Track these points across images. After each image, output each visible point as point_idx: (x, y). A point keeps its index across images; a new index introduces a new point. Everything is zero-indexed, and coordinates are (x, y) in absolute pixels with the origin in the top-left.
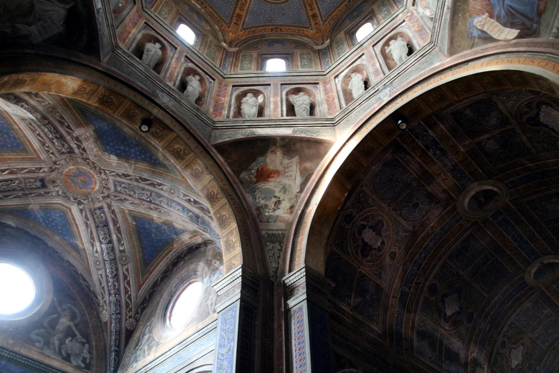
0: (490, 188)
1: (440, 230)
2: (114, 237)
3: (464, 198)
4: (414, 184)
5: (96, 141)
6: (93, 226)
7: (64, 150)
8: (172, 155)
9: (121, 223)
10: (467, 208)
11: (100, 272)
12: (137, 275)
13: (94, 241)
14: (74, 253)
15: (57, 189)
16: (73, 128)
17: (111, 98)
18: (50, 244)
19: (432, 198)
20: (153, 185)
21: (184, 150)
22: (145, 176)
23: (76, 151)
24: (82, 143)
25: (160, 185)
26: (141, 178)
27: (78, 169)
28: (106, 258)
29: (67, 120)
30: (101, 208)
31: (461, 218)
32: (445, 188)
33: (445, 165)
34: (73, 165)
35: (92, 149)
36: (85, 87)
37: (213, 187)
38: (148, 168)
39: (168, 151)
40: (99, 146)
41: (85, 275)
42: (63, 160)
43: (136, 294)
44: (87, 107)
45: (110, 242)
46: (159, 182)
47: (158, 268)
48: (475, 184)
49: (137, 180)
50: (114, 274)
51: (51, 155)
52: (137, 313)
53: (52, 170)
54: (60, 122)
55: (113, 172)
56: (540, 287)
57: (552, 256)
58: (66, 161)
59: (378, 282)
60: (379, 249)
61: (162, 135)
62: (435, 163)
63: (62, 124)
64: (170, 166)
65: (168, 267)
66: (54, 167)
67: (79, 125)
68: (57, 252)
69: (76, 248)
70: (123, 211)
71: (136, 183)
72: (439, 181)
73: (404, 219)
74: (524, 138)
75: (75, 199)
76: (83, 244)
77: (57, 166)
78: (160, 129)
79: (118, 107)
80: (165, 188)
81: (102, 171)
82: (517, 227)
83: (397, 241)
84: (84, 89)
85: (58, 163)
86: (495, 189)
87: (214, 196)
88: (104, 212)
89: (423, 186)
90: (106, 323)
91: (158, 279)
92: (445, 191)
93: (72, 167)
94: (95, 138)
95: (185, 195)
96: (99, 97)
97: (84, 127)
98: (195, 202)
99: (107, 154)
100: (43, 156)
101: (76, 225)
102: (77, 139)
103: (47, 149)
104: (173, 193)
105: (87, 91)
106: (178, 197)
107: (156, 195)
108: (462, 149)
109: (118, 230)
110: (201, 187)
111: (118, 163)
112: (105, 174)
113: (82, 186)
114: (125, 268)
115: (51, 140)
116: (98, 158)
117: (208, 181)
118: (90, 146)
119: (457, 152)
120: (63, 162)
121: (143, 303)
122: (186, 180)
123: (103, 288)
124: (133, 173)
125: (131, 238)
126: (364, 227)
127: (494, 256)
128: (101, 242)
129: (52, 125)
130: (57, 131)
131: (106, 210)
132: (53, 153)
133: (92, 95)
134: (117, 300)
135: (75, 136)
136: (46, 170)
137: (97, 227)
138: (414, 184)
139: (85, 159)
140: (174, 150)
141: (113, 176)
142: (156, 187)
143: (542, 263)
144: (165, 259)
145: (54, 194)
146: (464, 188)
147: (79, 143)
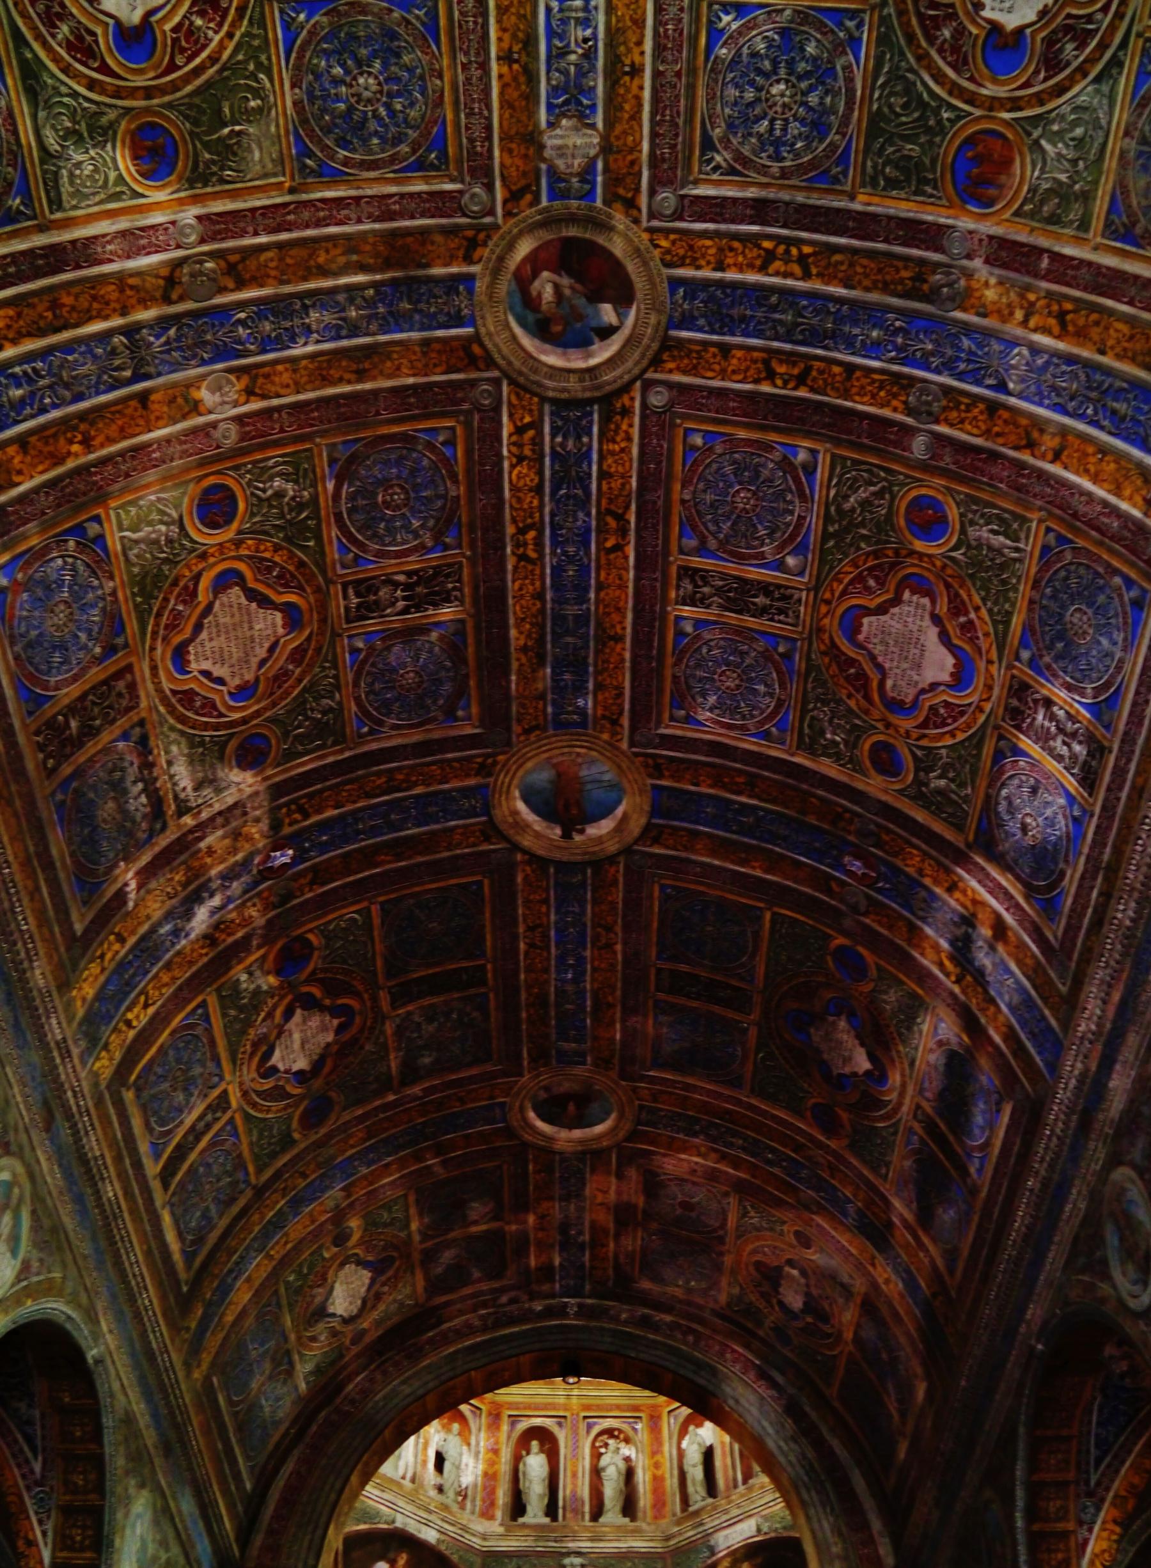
0: (540, 1124)
1: (695, 1134)
3: (599, 1137)
4: (654, 1226)
10: (613, 1116)
19: (652, 1184)
31: (641, 1107)
32: (613, 1180)
33: (580, 1209)
48: (558, 1146)
56: (632, 744)
57: (526, 842)
59: (859, 1300)
60: (803, 1273)
62: (594, 1226)
72: (612, 1196)
73: (725, 1220)
74: (414, 1226)
82: (552, 997)
83: (771, 1229)
86: (531, 1115)
89: (644, 1211)
92: (620, 1176)
108: (531, 1219)
119: (542, 1217)
126: (781, 1303)
127: (659, 971)
138: (654, 1226)
143: (566, 835)
146: (583, 1153)
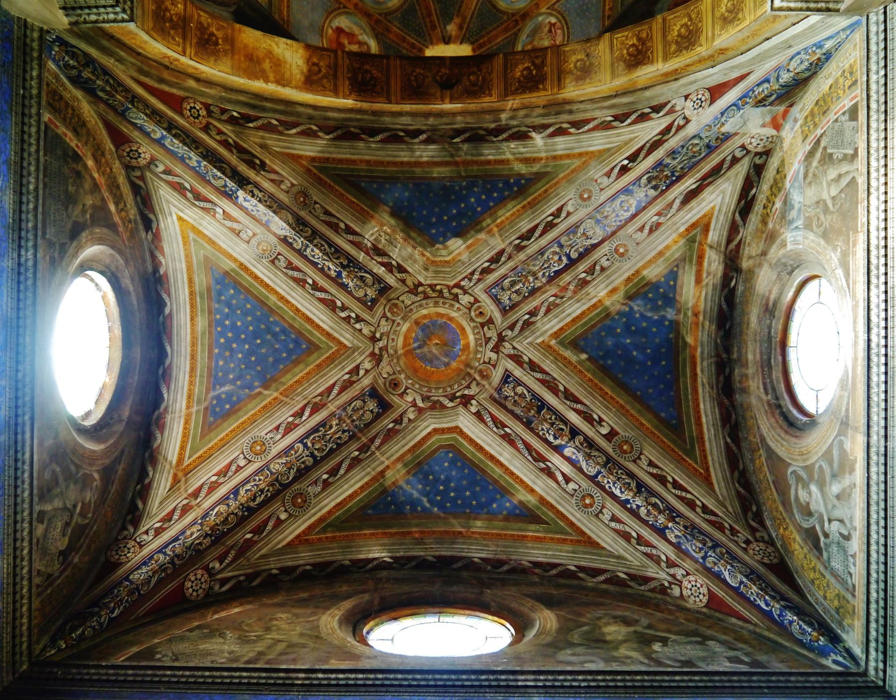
2: (574, 418)
5: (408, 238)
6: (519, 429)
7: (371, 293)
8: (524, 92)
9: (564, 380)
11: (606, 517)
12: (679, 462)
13: (544, 459)
14: (532, 531)
15: (409, 399)
16: (357, 229)
17: (367, 71)
18: (477, 553)
20: (550, 226)
21: (533, 63)
22: (525, 226)
23: (391, 280)
24: (390, 257)
25: (560, 210)
26: (522, 238)
27: (417, 323)
28: (592, 471)
29: (337, 215)
30: (507, 377)
34: (404, 319)
35: (411, 257)
36: (315, 60)
37: (622, 43)
38: (518, 207)
39: (512, 94)
40: (419, 239)
41: (588, 560)
42: (383, 322)
43: (717, 495)
44: (353, 170)
45: (574, 432)
46: (553, 209)
47: (704, 420)
49: (519, 248)
50: (633, 485)
51: (358, 326)
52: (753, 531)
53: (377, 359)
54: (329, 224)
55: (472, 273)
58: (387, 319)
61: (484, 79)
63: (335, 227)
64: (546, 166)
65: (721, 405)
66: (377, 351)
67: (364, 217)
68: (501, 563)
69: (527, 515)
70: (545, 347)
71: (522, 256)
75: (452, 398)
76: (532, 491)
77: (381, 344)
78: (473, 73)
79: (388, 83)
80: (570, 208)
81: (455, 290)
84: (316, 68)
85: (378, 335)
87: (637, 49)
88: (519, 382)
90: (713, 601)
91: (726, 443)
93: (405, 327)
94: (402, 230)
95: (608, 175)
96: (348, 78)
97: (372, 217)
98: (633, 158)
99: (440, 246)
100: (346, 337)
101: (492, 458)
102: (378, 251)
103: (343, 315)
104: (589, 198)
105: (324, 71)
106: (602, 190)
107: (568, 235)
109: (569, 396)
110: (609, 73)
111: (468, 247)
112: (465, 292)
113: (446, 360)
114: (644, 463)
115: (336, 280)
116: (432, 269)
117: (608, 51)
118: (404, 253)
120: (385, 327)
121: (745, 509)
122: (587, 153)
123: (640, 540)
124: (503, 241)
125: (604, 395)
128: (558, 449)
129: (321, 238)
130: (337, 251)
131: (518, 372)
132: (359, 319)
133: (335, 77)
134: (686, 527)
135: (369, 245)
136: (367, 365)
137: (528, 424)
139: (414, 290)
140: (519, 82)
141: (479, 280)
142: (556, 224)
144: (700, 391)
145: (412, 416)
147: (385, 260)
